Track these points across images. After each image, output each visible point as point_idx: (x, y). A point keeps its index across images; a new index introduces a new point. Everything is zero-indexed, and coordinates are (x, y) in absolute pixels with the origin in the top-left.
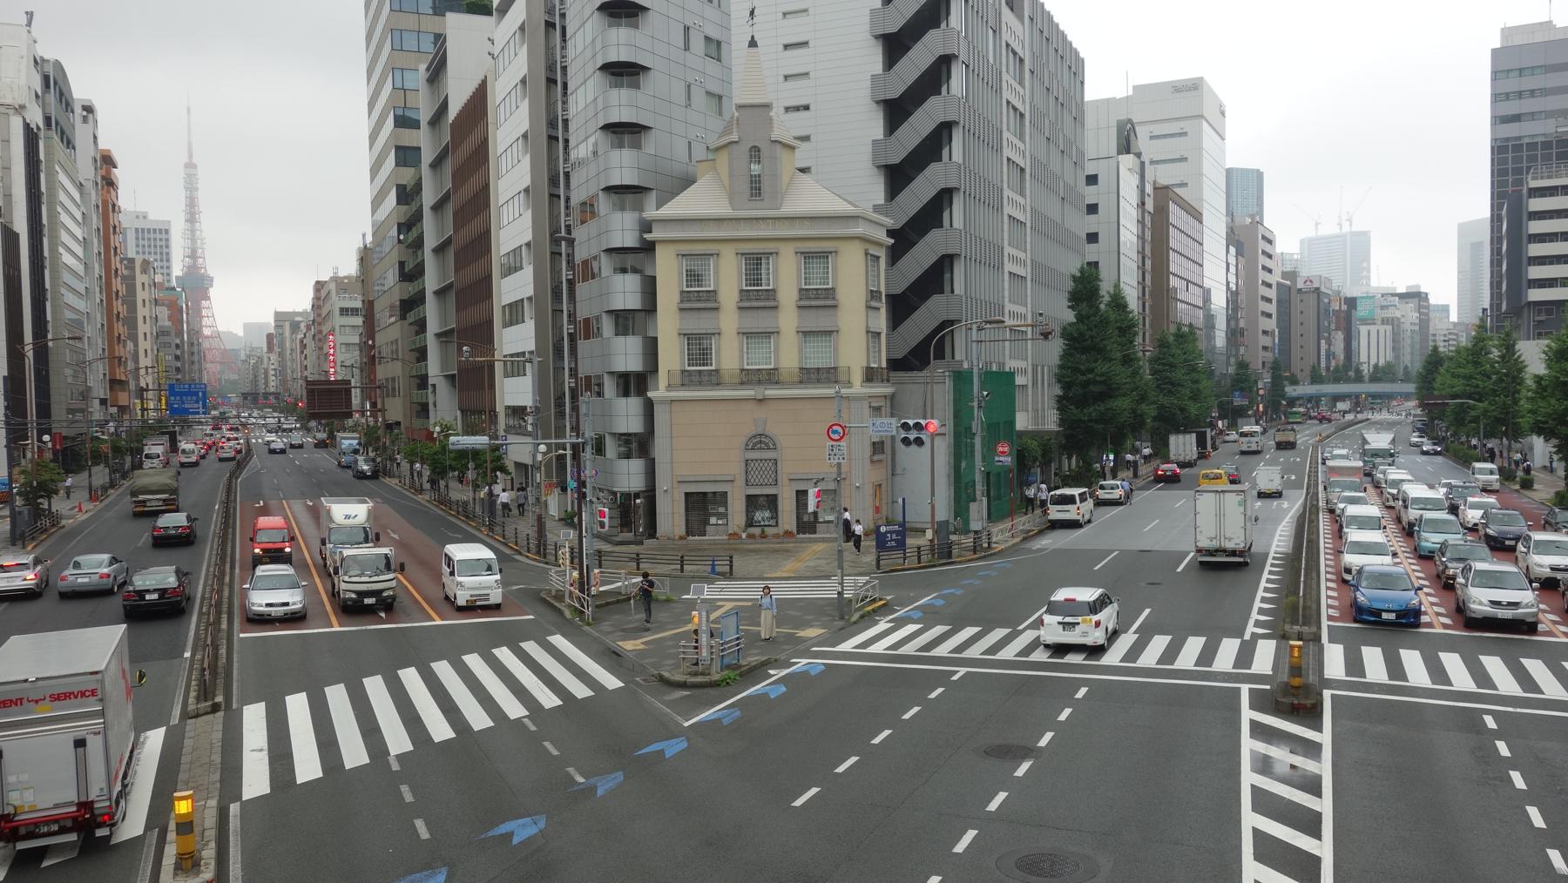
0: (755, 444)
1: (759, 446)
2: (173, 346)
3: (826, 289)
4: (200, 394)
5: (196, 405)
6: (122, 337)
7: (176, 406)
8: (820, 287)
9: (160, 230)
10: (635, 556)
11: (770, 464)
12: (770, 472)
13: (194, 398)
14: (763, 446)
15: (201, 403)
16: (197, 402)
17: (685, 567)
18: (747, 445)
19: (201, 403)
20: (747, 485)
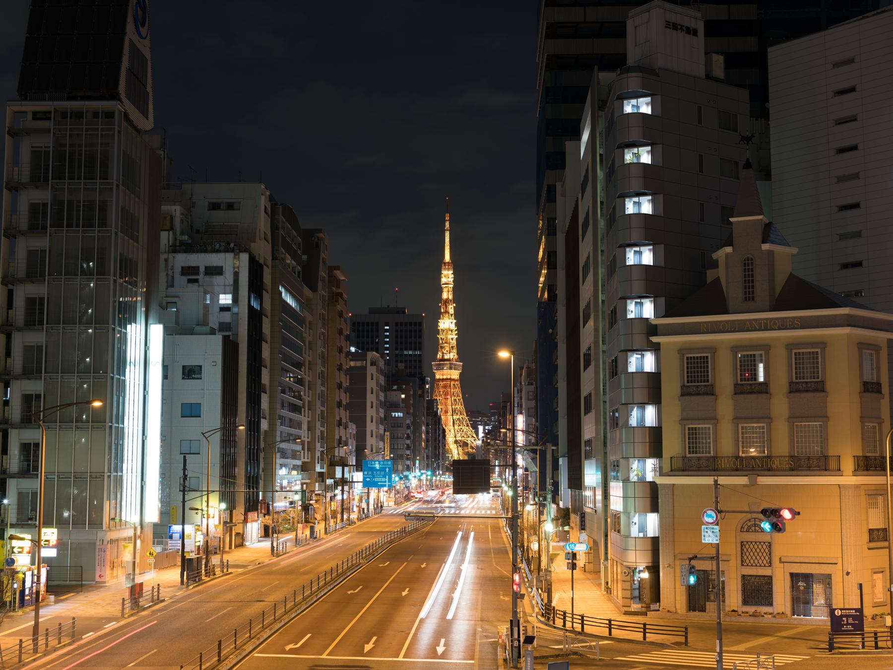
0: (750, 527)
1: (753, 528)
2: (405, 426)
3: (706, 386)
4: (387, 470)
5: (383, 480)
6: (344, 420)
7: (368, 479)
8: (700, 384)
9: (415, 323)
10: (684, 630)
11: (764, 547)
12: (765, 554)
13: (382, 473)
14: (757, 528)
15: (387, 477)
16: (384, 477)
17: (647, 635)
18: (742, 527)
19: (387, 477)
20: (742, 565)
